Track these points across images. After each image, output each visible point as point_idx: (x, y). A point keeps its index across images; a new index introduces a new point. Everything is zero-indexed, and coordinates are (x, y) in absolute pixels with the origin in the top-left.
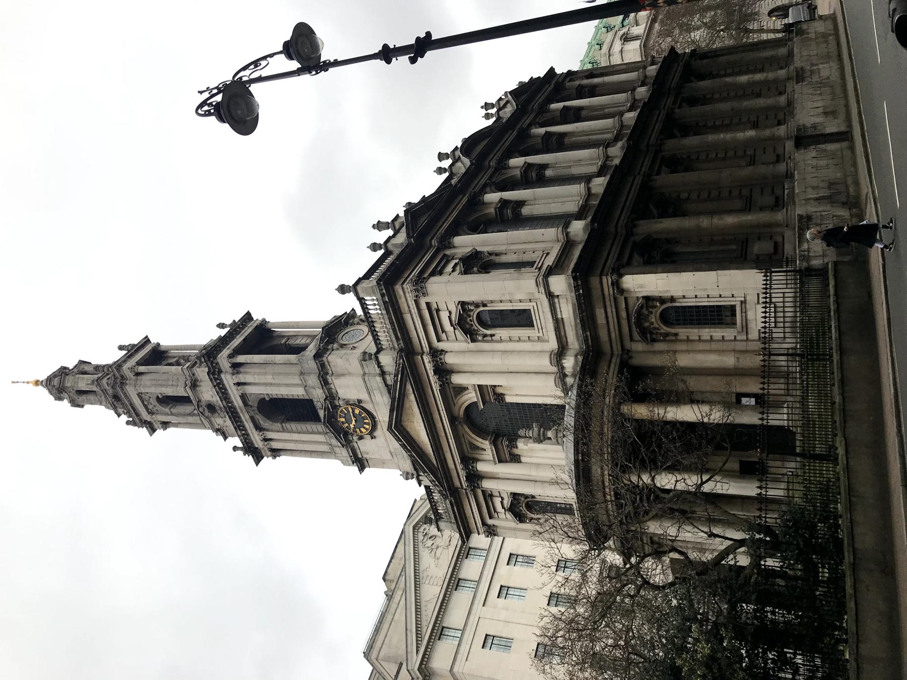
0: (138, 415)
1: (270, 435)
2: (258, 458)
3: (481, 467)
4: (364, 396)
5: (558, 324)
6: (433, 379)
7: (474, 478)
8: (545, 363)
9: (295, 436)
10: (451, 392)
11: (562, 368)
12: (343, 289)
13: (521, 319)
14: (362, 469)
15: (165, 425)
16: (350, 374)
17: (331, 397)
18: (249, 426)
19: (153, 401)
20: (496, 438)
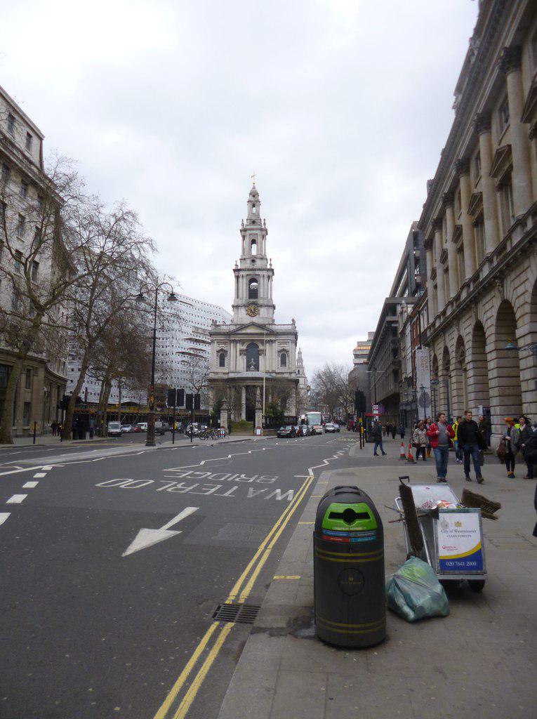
0: (250, 230)
1: (245, 279)
2: (235, 270)
3: (238, 344)
4: (261, 316)
5: (283, 373)
6: (268, 339)
7: (235, 342)
8: (274, 369)
9: (245, 288)
10: (262, 342)
11: (272, 373)
12: (293, 320)
13: (283, 362)
14: (233, 306)
15: (244, 237)
16: (268, 313)
17: (261, 306)
18: (249, 273)
19: (253, 238)
20: (246, 350)
